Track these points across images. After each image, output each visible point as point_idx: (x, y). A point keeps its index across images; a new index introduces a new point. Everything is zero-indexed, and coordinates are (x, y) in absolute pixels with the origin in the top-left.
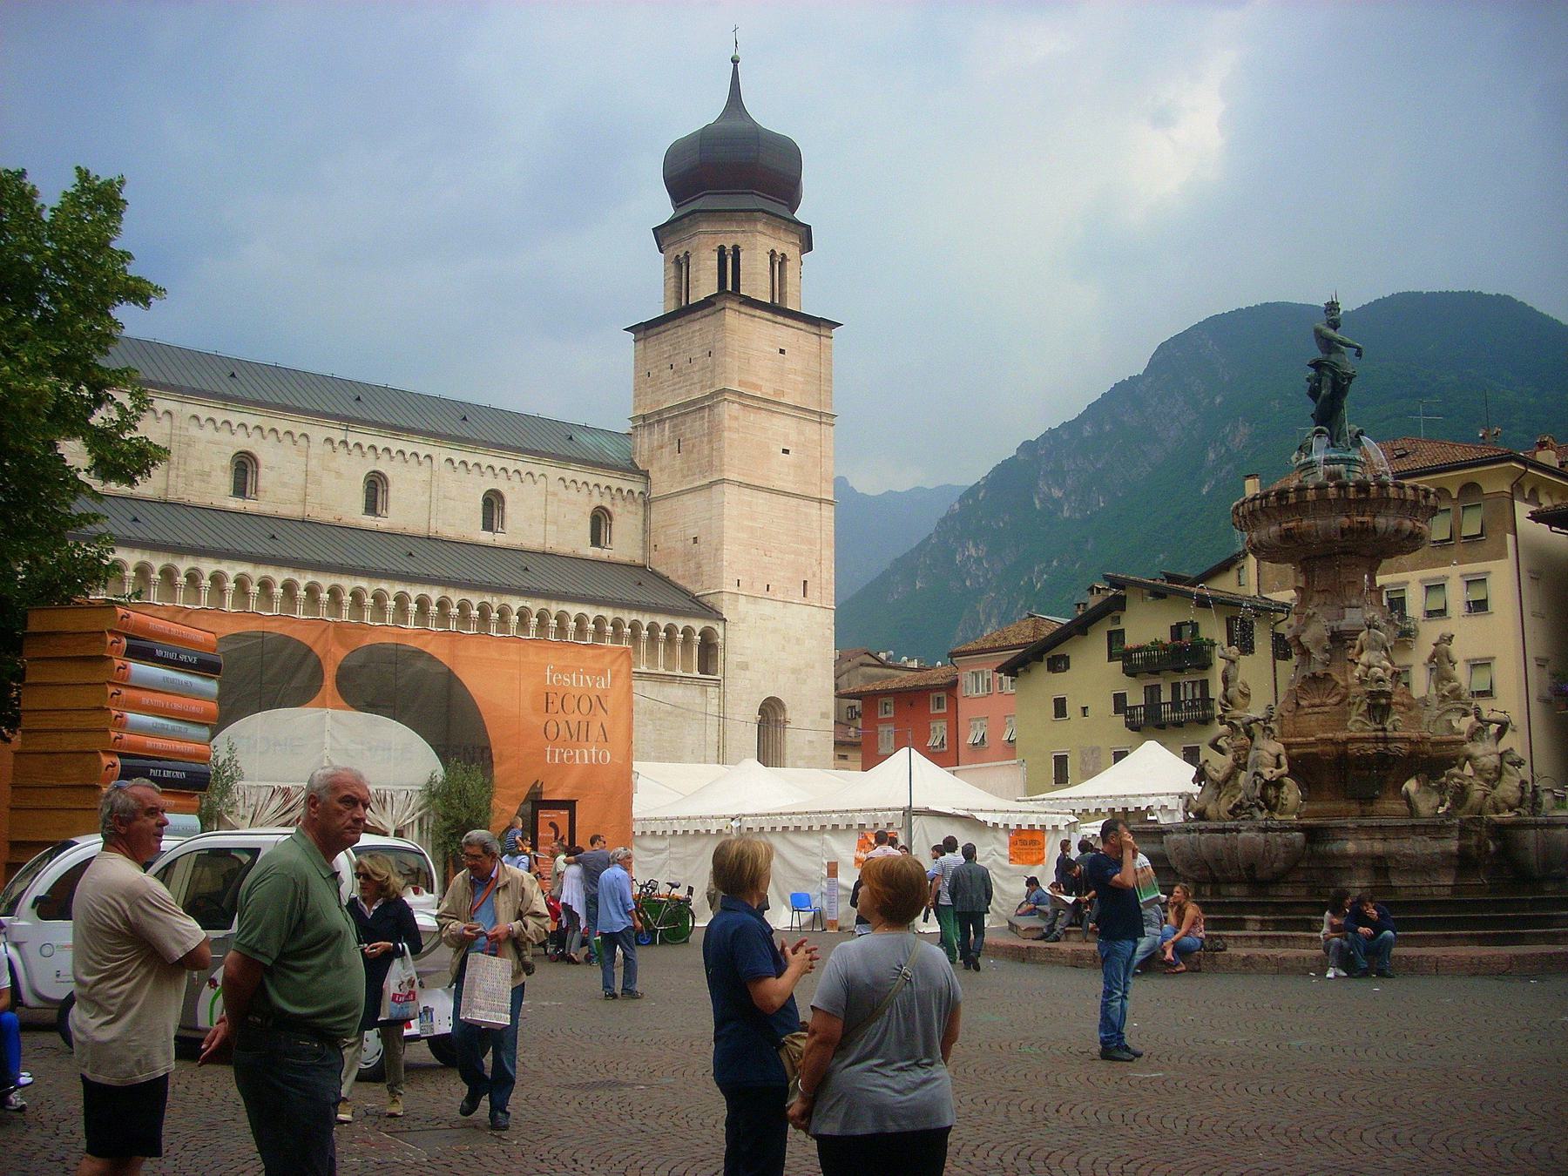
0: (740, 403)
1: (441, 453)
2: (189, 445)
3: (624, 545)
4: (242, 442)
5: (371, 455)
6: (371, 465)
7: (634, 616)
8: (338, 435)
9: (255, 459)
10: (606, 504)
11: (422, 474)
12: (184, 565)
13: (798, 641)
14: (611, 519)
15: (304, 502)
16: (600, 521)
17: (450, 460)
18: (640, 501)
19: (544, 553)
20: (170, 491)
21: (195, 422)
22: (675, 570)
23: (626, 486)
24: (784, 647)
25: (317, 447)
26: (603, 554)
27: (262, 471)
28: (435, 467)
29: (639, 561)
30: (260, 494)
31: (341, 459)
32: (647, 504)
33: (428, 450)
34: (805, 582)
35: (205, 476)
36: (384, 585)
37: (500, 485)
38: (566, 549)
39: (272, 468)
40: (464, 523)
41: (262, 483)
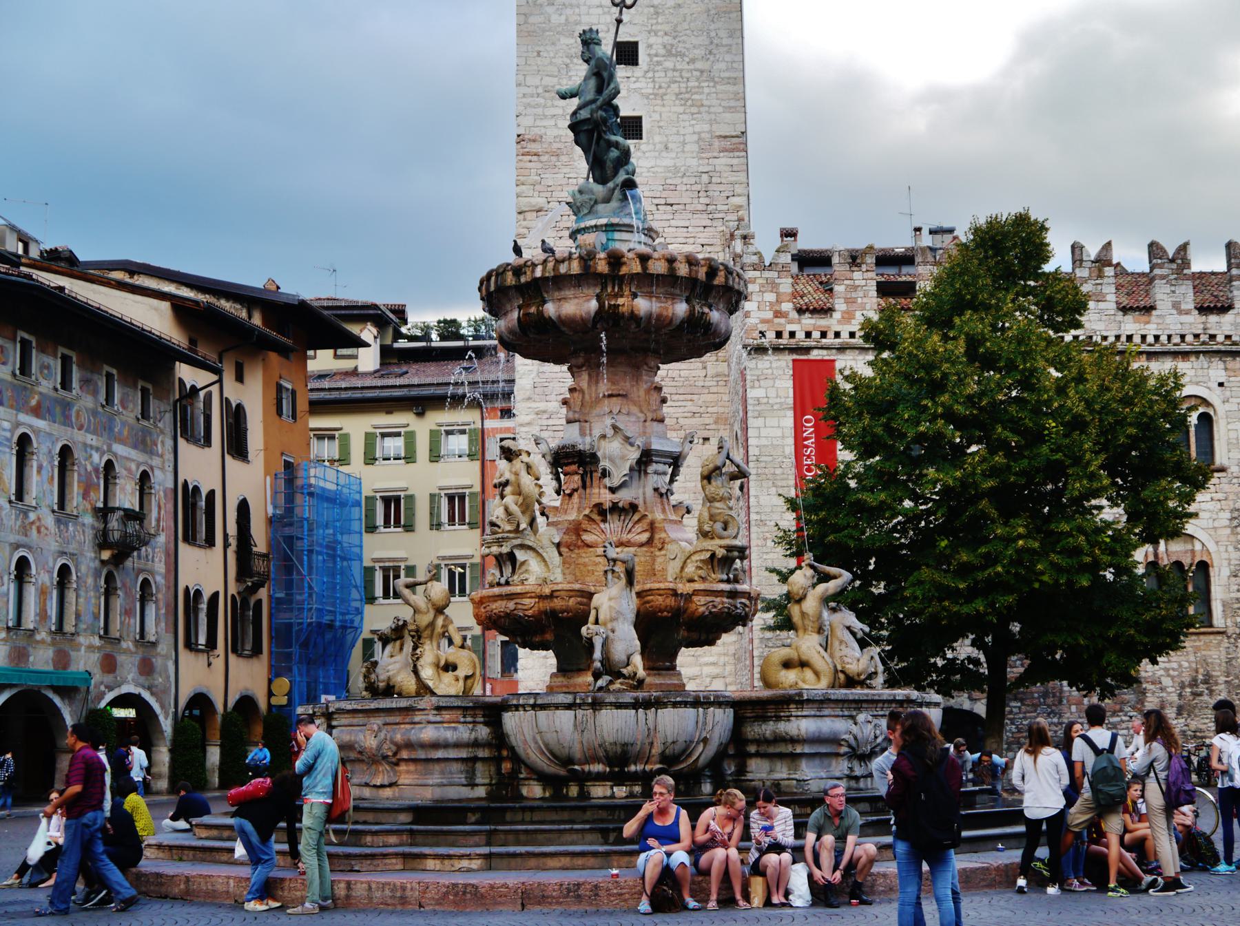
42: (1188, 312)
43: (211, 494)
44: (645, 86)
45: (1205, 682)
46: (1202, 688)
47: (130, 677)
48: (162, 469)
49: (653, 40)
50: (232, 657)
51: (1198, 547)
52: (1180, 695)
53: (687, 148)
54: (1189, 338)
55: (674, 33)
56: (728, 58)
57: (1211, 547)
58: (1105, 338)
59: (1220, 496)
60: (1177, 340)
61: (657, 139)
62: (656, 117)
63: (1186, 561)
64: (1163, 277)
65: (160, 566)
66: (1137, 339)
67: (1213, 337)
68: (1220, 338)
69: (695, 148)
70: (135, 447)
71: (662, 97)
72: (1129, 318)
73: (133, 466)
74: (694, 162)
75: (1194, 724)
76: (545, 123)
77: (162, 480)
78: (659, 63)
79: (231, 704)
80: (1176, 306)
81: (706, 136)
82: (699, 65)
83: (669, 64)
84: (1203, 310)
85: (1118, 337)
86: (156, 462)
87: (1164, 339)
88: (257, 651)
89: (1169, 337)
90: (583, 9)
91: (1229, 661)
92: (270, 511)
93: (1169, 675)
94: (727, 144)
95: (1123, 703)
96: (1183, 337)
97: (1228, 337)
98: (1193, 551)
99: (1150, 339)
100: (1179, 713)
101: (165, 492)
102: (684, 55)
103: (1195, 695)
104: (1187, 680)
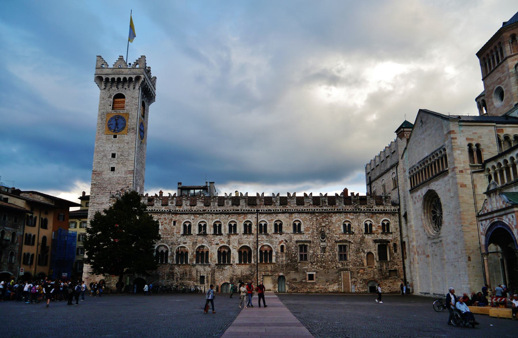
42: (188, 206)
43: (34, 236)
44: (116, 162)
45: (185, 274)
46: (185, 275)
47: (5, 270)
48: (20, 231)
49: (118, 153)
50: (38, 266)
51: (186, 249)
52: (180, 276)
53: (123, 173)
54: (188, 211)
55: (122, 152)
56: (131, 156)
57: (188, 249)
58: (173, 211)
59: (191, 239)
60: (186, 211)
61: (117, 171)
62: (118, 167)
63: (184, 251)
64: (184, 199)
65: (17, 249)
66: (179, 211)
67: (192, 210)
68: (194, 211)
69: (124, 173)
70: (12, 227)
71: (119, 163)
72: (177, 207)
73: (11, 231)
74: (123, 175)
75: (182, 281)
76: (98, 168)
77: (19, 233)
78: (119, 157)
79: (37, 274)
80: (186, 205)
81: (126, 171)
82: (126, 158)
83: (121, 158)
84: (191, 206)
85: (175, 210)
86: (18, 230)
87: (183, 211)
88: (46, 265)
89: (184, 210)
90: (106, 147)
91: (190, 270)
92: (53, 238)
93: (179, 272)
94: (130, 172)
95: (170, 277)
96: (187, 210)
97: (195, 210)
98: (185, 250)
99: (181, 211)
100: (180, 280)
101: (20, 236)
102: (123, 156)
103: (183, 276)
104: (182, 273)
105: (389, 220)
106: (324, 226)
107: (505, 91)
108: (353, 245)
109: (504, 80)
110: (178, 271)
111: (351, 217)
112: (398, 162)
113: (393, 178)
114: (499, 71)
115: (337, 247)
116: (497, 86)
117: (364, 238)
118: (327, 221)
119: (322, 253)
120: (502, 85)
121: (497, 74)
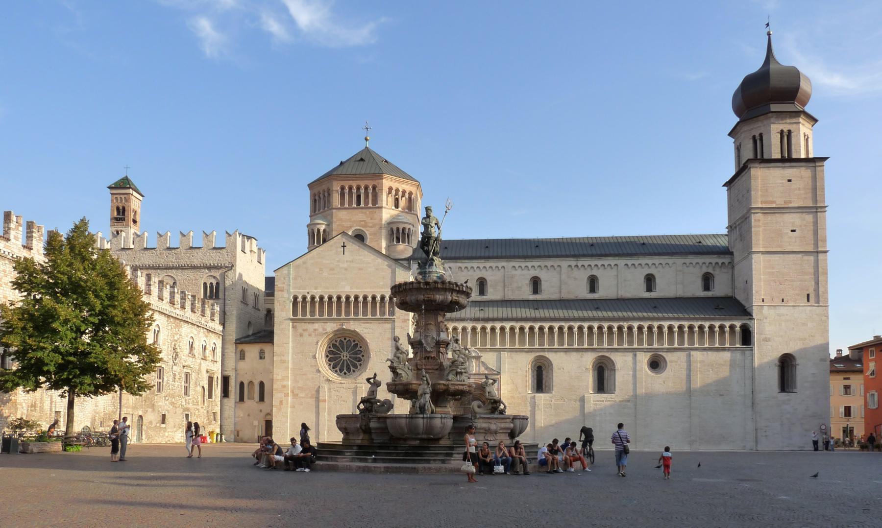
0: (763, 213)
1: (621, 262)
2: (512, 278)
3: (720, 289)
4: (533, 273)
5: (589, 269)
6: (590, 273)
7: (700, 323)
8: (573, 263)
9: (540, 279)
10: (710, 270)
11: (614, 272)
12: (489, 326)
13: (804, 324)
14: (714, 277)
15: (560, 292)
16: (707, 280)
17: (627, 265)
18: (730, 266)
19: (676, 298)
20: (506, 296)
21: (514, 269)
22: (740, 297)
23: (720, 261)
24: (793, 329)
25: (565, 269)
26: (709, 294)
27: (542, 283)
28: (619, 268)
29: (730, 294)
30: (542, 291)
31: (576, 273)
32: (733, 267)
33: (616, 262)
34: (808, 295)
35: (519, 288)
36: (572, 324)
37: (652, 271)
38: (689, 294)
39: (546, 281)
40: (636, 289)
41: (543, 288)
105: (216, 343)
106: (176, 341)
107: (370, 238)
108: (193, 373)
109: (371, 227)
110: (24, 400)
111: (195, 332)
112: (233, 266)
113: (205, 284)
114: (365, 213)
115: (183, 375)
116: (358, 228)
117: (200, 364)
118: (178, 332)
119: (173, 382)
120: (367, 230)
121: (361, 214)
